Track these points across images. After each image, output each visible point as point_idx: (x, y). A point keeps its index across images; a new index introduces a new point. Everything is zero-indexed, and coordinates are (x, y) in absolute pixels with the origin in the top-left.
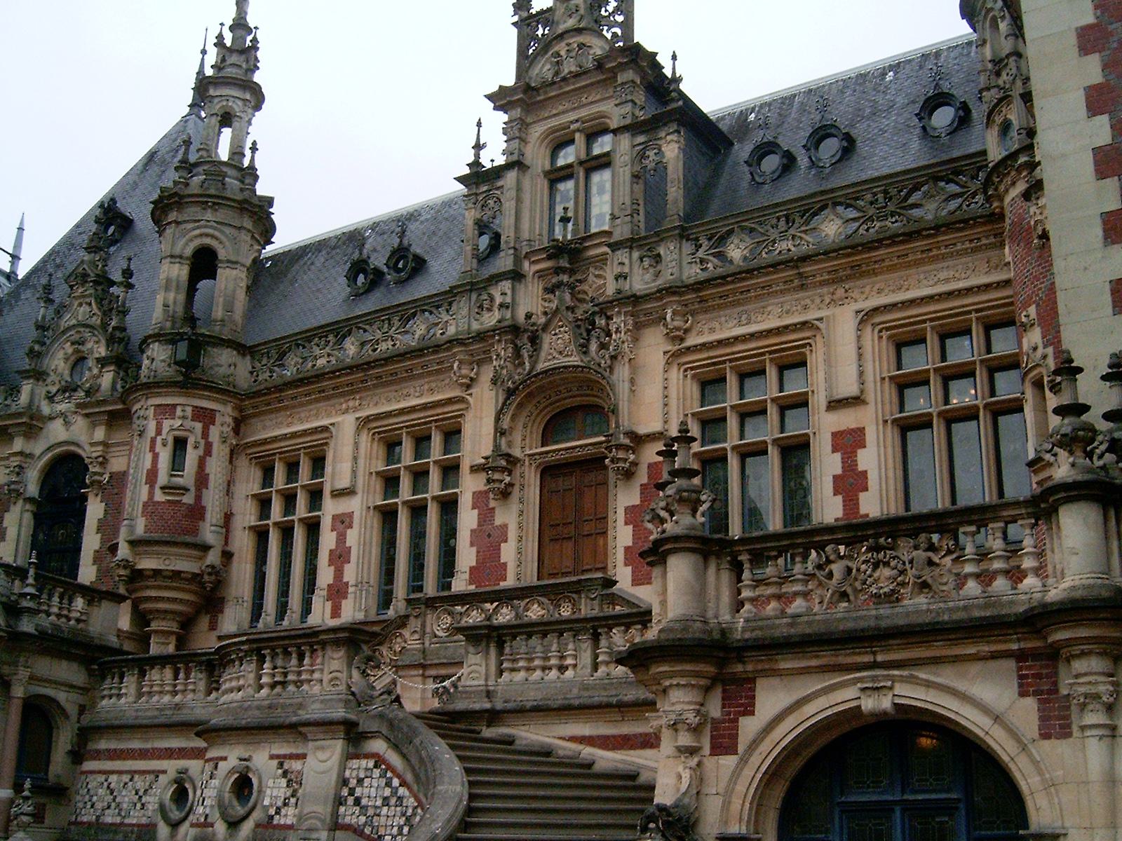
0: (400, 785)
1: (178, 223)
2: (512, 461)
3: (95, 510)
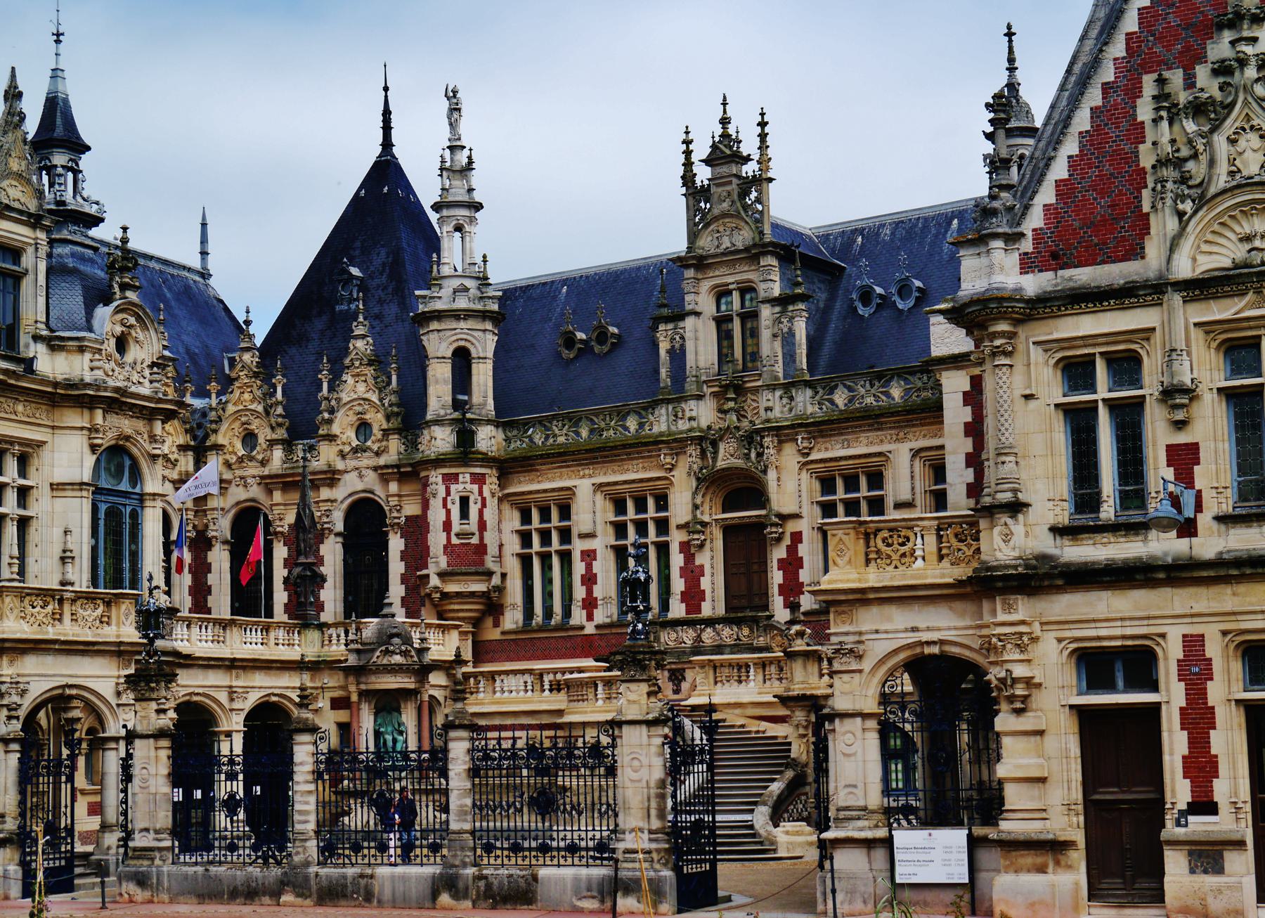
2: (705, 524)
3: (396, 544)
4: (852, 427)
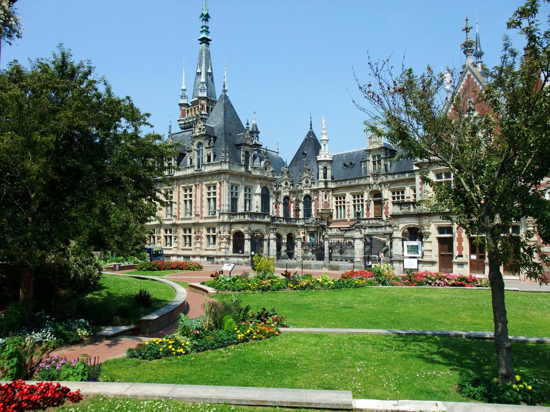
3: (313, 204)
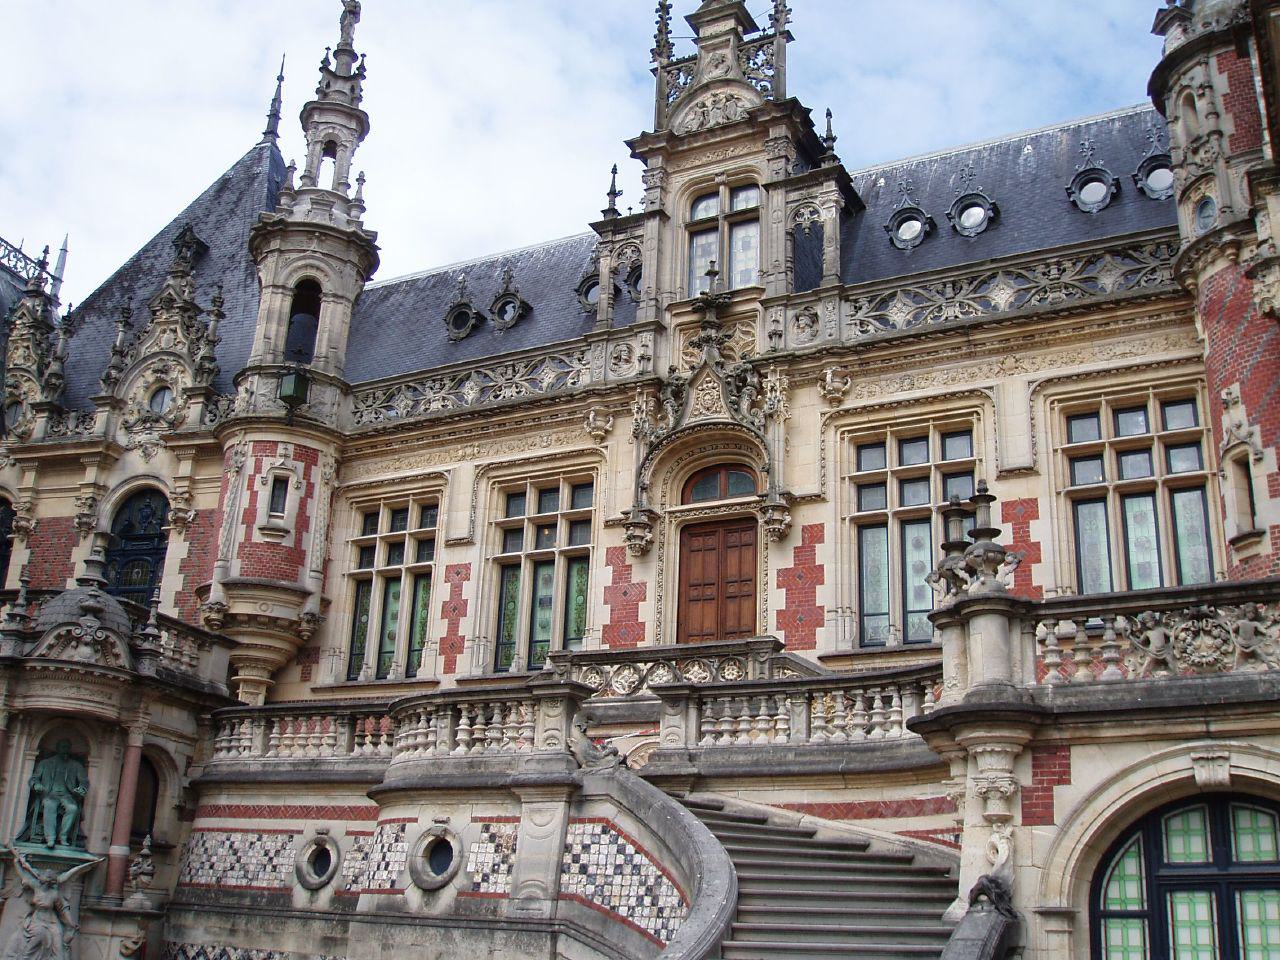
0: (636, 852)
1: (281, 252)
2: (653, 517)
3: (177, 548)
4: (921, 352)
